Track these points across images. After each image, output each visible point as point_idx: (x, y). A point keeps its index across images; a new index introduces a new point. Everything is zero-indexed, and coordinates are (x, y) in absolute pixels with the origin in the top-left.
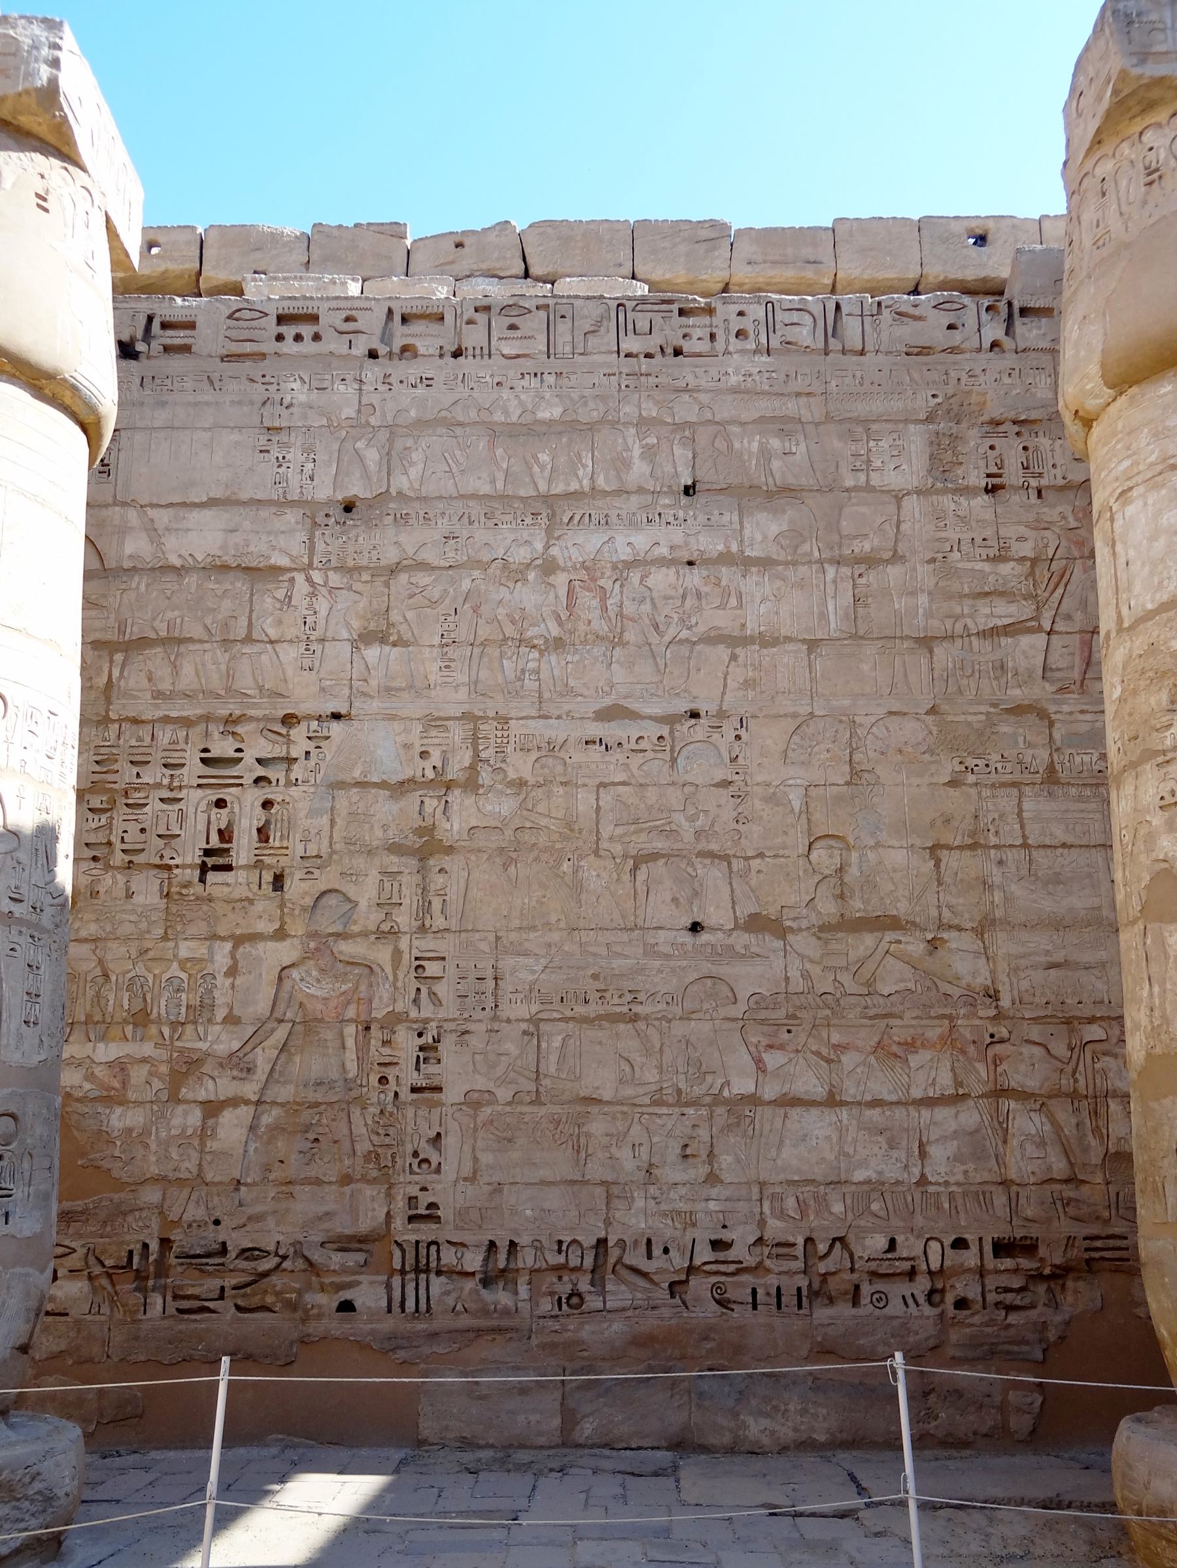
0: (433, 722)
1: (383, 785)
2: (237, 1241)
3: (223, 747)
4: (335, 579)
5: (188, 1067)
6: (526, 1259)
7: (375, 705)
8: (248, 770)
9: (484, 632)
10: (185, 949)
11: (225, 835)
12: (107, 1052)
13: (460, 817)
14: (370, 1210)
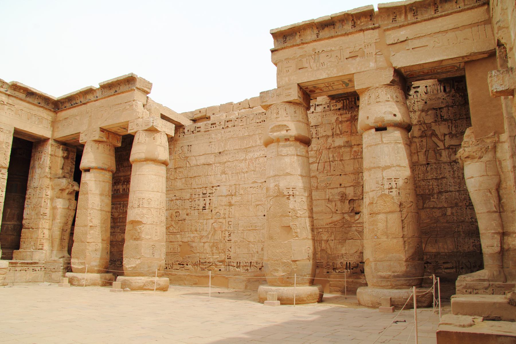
0: (230, 186)
1: (224, 196)
2: (208, 261)
3: (205, 192)
4: (218, 165)
5: (202, 237)
6: (241, 264)
7: (223, 184)
8: (208, 195)
9: (238, 171)
10: (201, 221)
11: (205, 204)
12: (192, 235)
13: (234, 200)
14: (223, 257)
